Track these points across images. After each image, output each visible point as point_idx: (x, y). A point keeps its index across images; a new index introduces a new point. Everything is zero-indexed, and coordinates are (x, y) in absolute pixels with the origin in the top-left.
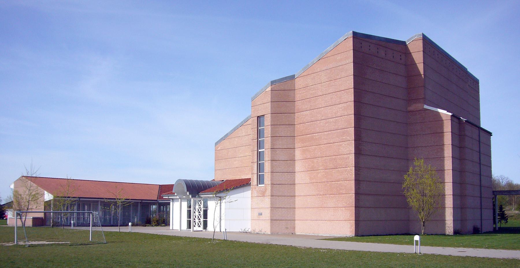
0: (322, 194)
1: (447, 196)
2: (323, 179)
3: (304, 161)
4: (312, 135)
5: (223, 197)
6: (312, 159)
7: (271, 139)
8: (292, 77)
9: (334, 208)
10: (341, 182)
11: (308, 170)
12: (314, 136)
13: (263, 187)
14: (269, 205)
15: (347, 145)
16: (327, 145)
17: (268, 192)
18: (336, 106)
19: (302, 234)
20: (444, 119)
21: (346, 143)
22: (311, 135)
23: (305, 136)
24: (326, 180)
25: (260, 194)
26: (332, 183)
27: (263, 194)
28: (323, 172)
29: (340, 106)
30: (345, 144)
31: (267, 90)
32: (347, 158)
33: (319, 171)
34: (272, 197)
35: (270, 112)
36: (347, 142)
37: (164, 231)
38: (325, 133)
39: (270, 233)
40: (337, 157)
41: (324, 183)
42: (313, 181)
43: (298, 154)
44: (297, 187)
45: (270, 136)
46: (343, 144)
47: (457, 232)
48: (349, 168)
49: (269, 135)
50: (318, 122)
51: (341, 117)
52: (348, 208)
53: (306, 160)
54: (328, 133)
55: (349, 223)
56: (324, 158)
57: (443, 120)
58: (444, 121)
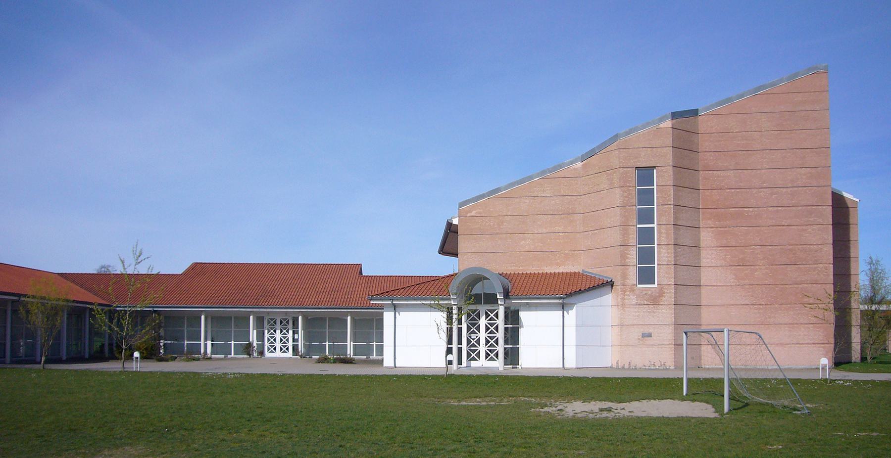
0: (763, 303)
1: (853, 310)
2: (767, 280)
3: (721, 250)
4: (741, 209)
5: (567, 304)
6: (741, 248)
7: (674, 209)
8: (694, 113)
9: (791, 326)
10: (805, 285)
11: (731, 264)
12: (745, 211)
13: (653, 290)
14: (670, 319)
15: (818, 230)
16: (775, 228)
17: (669, 296)
18: (793, 170)
19: (716, 367)
20: (849, 205)
21: (815, 227)
22: (737, 209)
23: (723, 210)
24: (772, 281)
25: (645, 300)
26: (786, 287)
27: (655, 300)
28: (767, 269)
29: (803, 171)
30: (813, 230)
31: (662, 125)
32: (816, 251)
33: (757, 267)
34: (675, 306)
35: (671, 164)
36: (818, 226)
37: (92, 367)
38: (770, 209)
39: (673, 368)
40: (796, 246)
41: (768, 286)
42: (742, 282)
43: (706, 237)
44: (703, 291)
45: (672, 203)
46: (810, 228)
47: (863, 359)
48: (821, 266)
49: (669, 200)
50: (755, 191)
51: (805, 188)
52: (820, 325)
53: (728, 248)
54: (775, 209)
55: (823, 347)
56: (767, 247)
57: (848, 208)
58: (850, 209)
